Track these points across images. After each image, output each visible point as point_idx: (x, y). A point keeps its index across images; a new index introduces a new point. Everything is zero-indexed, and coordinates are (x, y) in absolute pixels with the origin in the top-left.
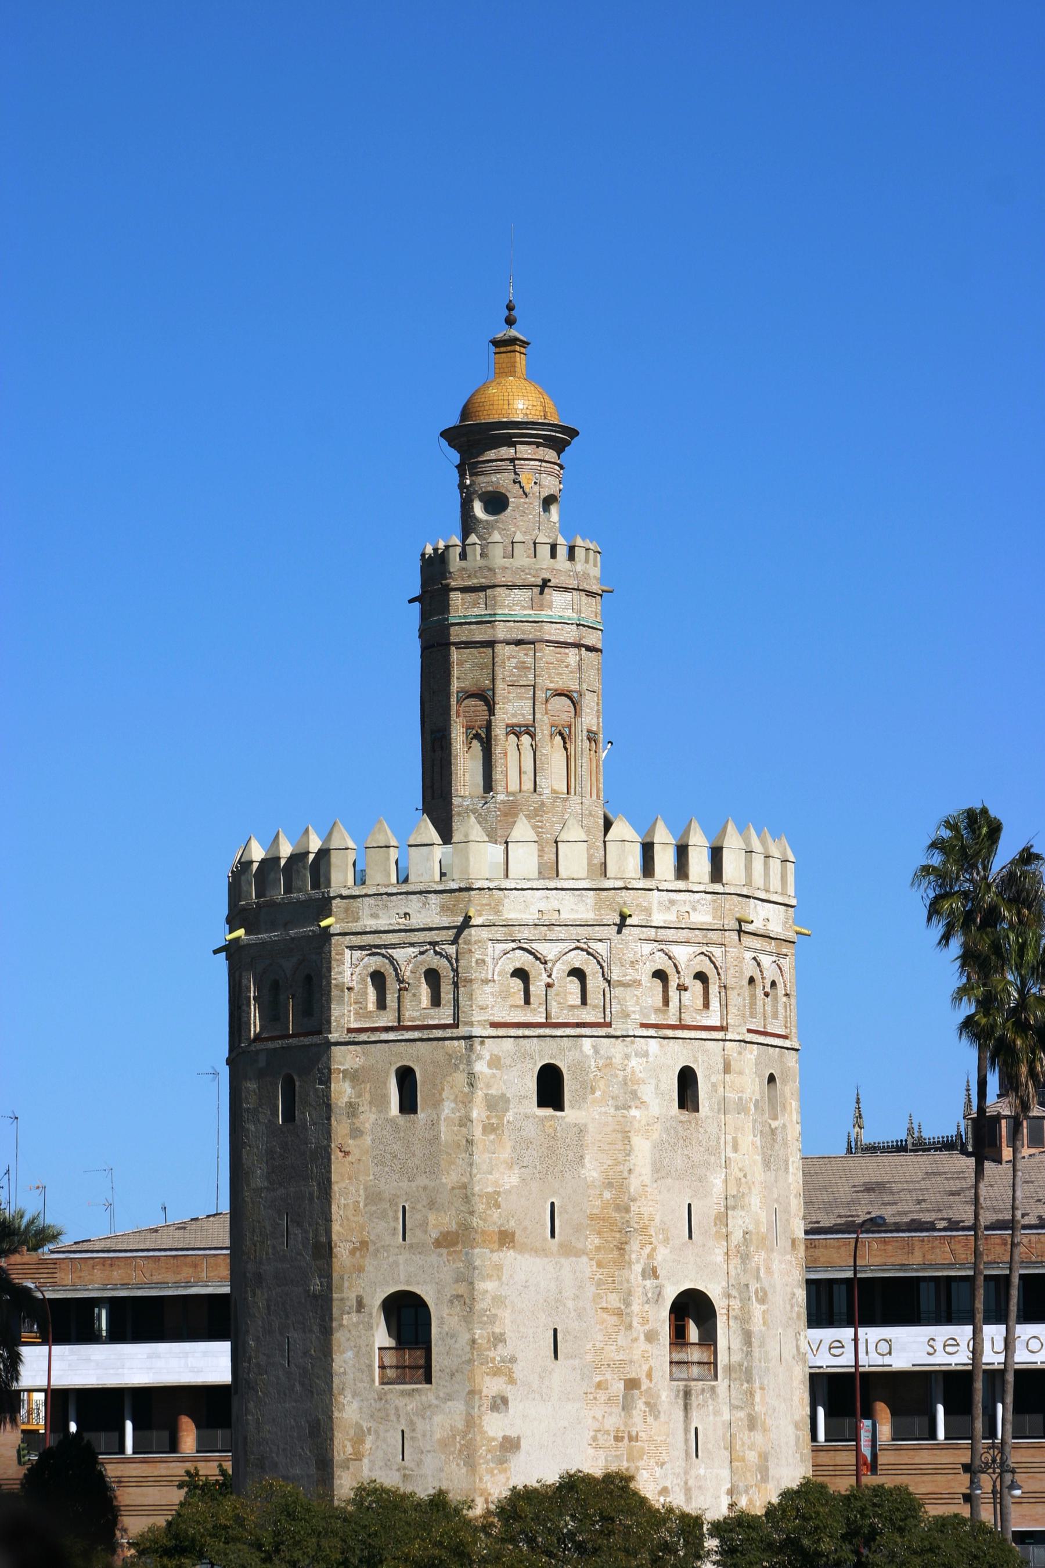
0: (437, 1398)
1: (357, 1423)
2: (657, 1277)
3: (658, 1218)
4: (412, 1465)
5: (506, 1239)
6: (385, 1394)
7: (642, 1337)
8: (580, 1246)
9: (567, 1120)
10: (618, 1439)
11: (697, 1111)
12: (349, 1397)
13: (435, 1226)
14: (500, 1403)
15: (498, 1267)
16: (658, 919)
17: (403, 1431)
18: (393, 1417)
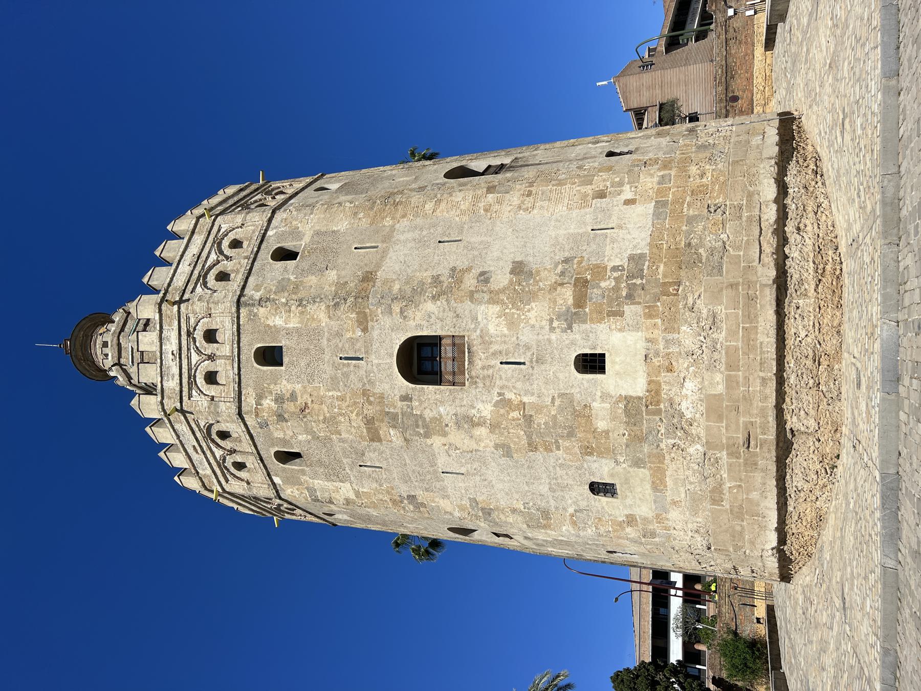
0: (475, 330)
1: (494, 406)
4: (529, 354)
5: (368, 278)
6: (471, 377)
8: (388, 229)
10: (529, 194)
12: (474, 411)
13: (354, 332)
14: (484, 278)
15: (385, 281)
17: (501, 363)
18: (491, 371)
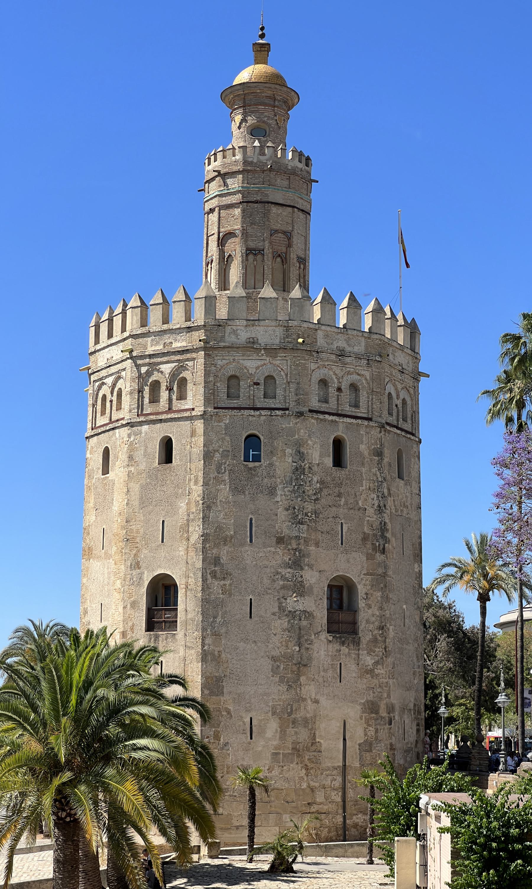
2: (139, 568)
3: (142, 531)
7: (129, 606)
9: (110, 478)
11: (171, 462)
16: (150, 350)
